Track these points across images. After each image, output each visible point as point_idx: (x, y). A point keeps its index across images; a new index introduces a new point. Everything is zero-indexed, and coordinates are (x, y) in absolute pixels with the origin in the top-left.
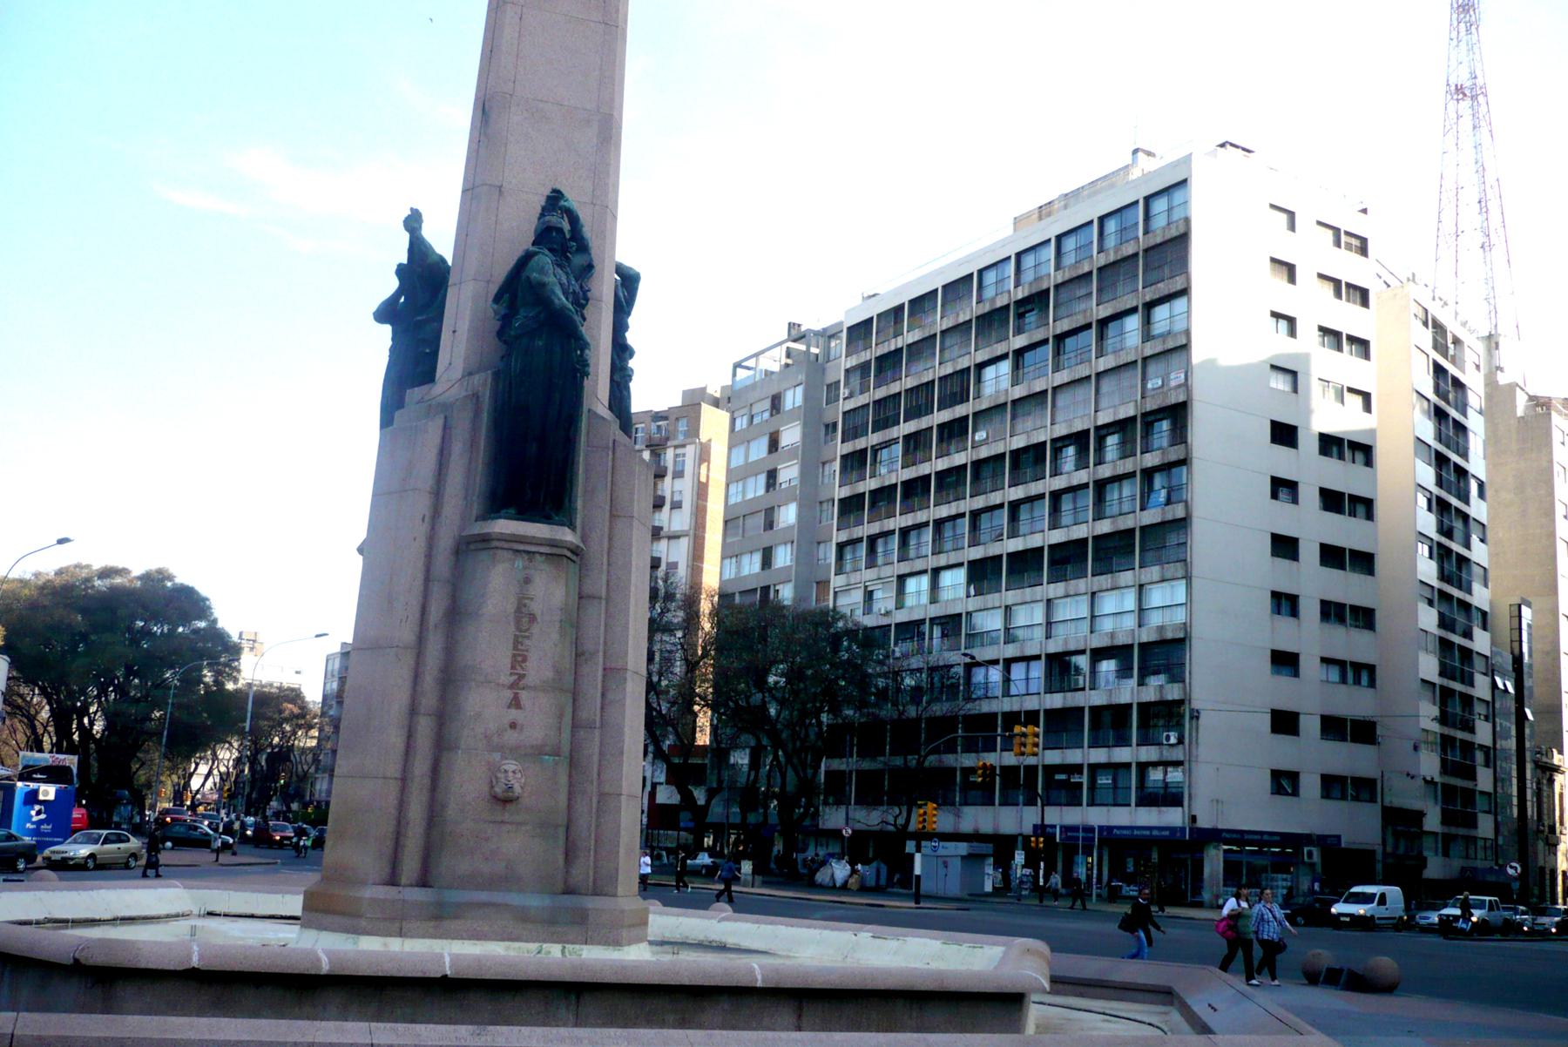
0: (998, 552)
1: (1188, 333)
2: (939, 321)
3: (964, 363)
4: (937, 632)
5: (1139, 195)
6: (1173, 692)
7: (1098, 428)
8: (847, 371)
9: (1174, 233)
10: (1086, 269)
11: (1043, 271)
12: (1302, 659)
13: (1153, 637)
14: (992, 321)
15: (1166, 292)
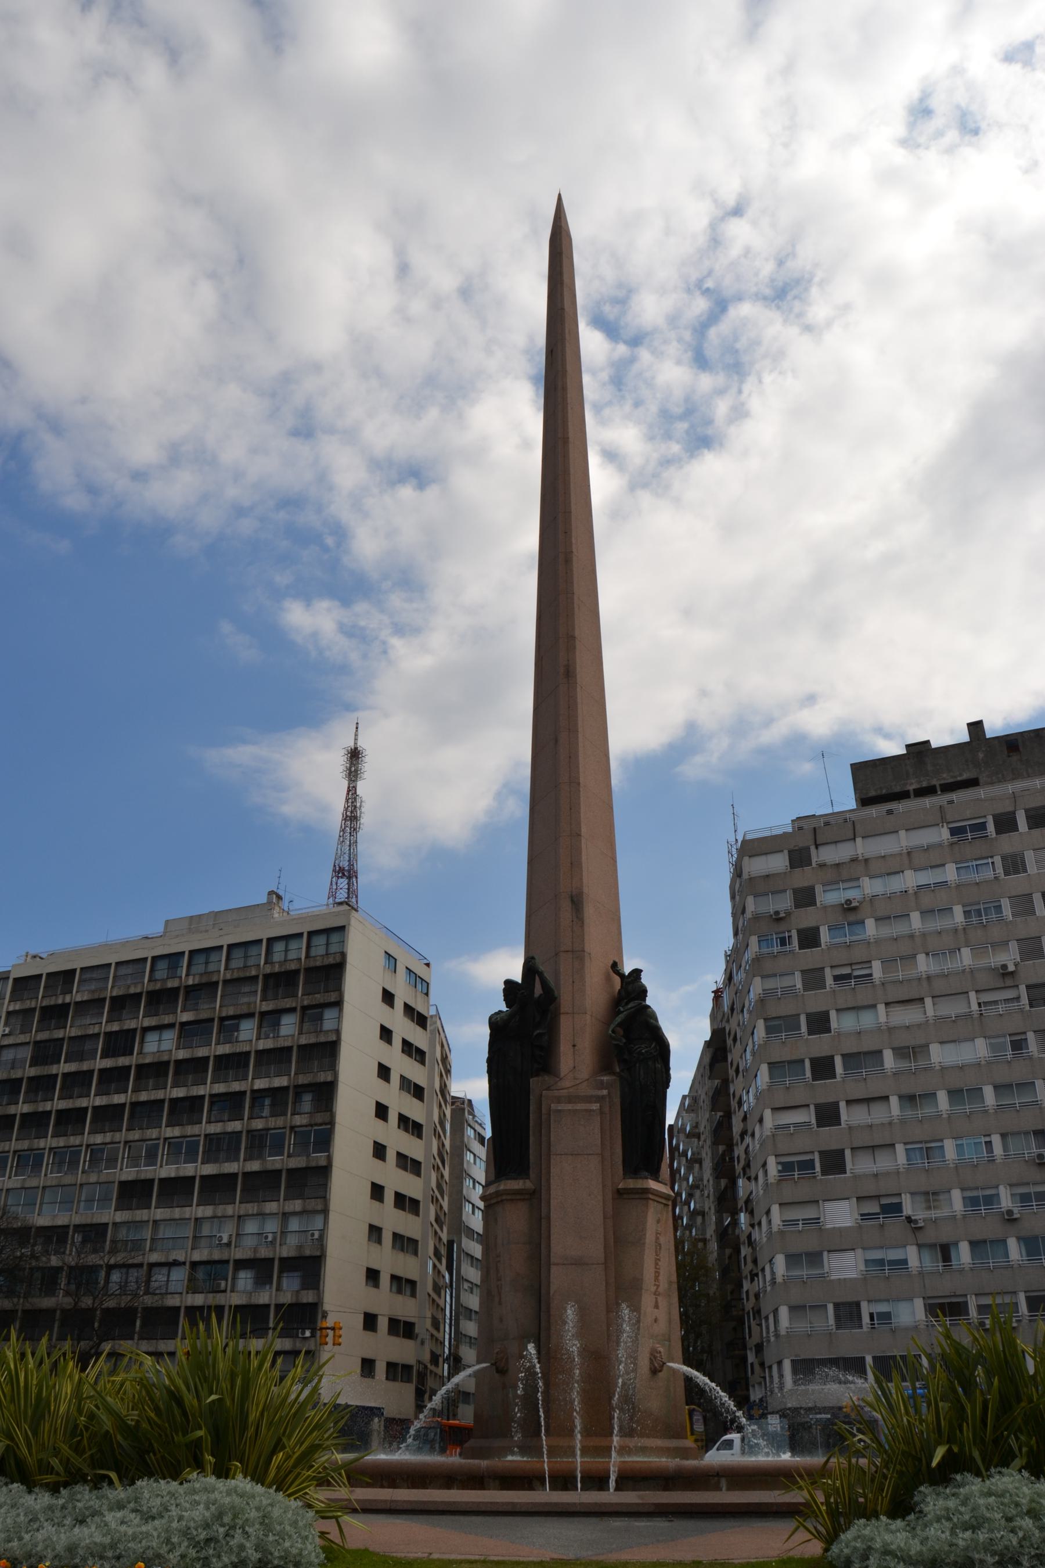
0: (149, 1176)
1: (338, 1032)
3: (131, 1024)
4: (78, 1238)
5: (305, 929)
6: (308, 1297)
8: (9, 1013)
9: (331, 960)
10: (254, 973)
11: (212, 968)
12: (382, 1274)
13: (292, 1254)
15: (322, 1001)
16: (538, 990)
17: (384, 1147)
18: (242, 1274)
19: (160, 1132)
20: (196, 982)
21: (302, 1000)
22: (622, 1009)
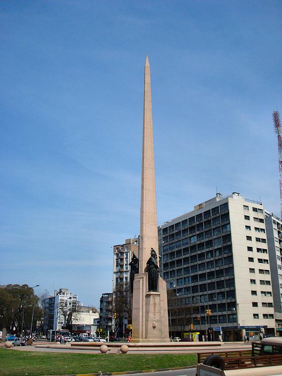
1: (230, 231)
2: (181, 228)
6: (233, 300)
14: (192, 229)
17: (253, 258)
18: (219, 296)
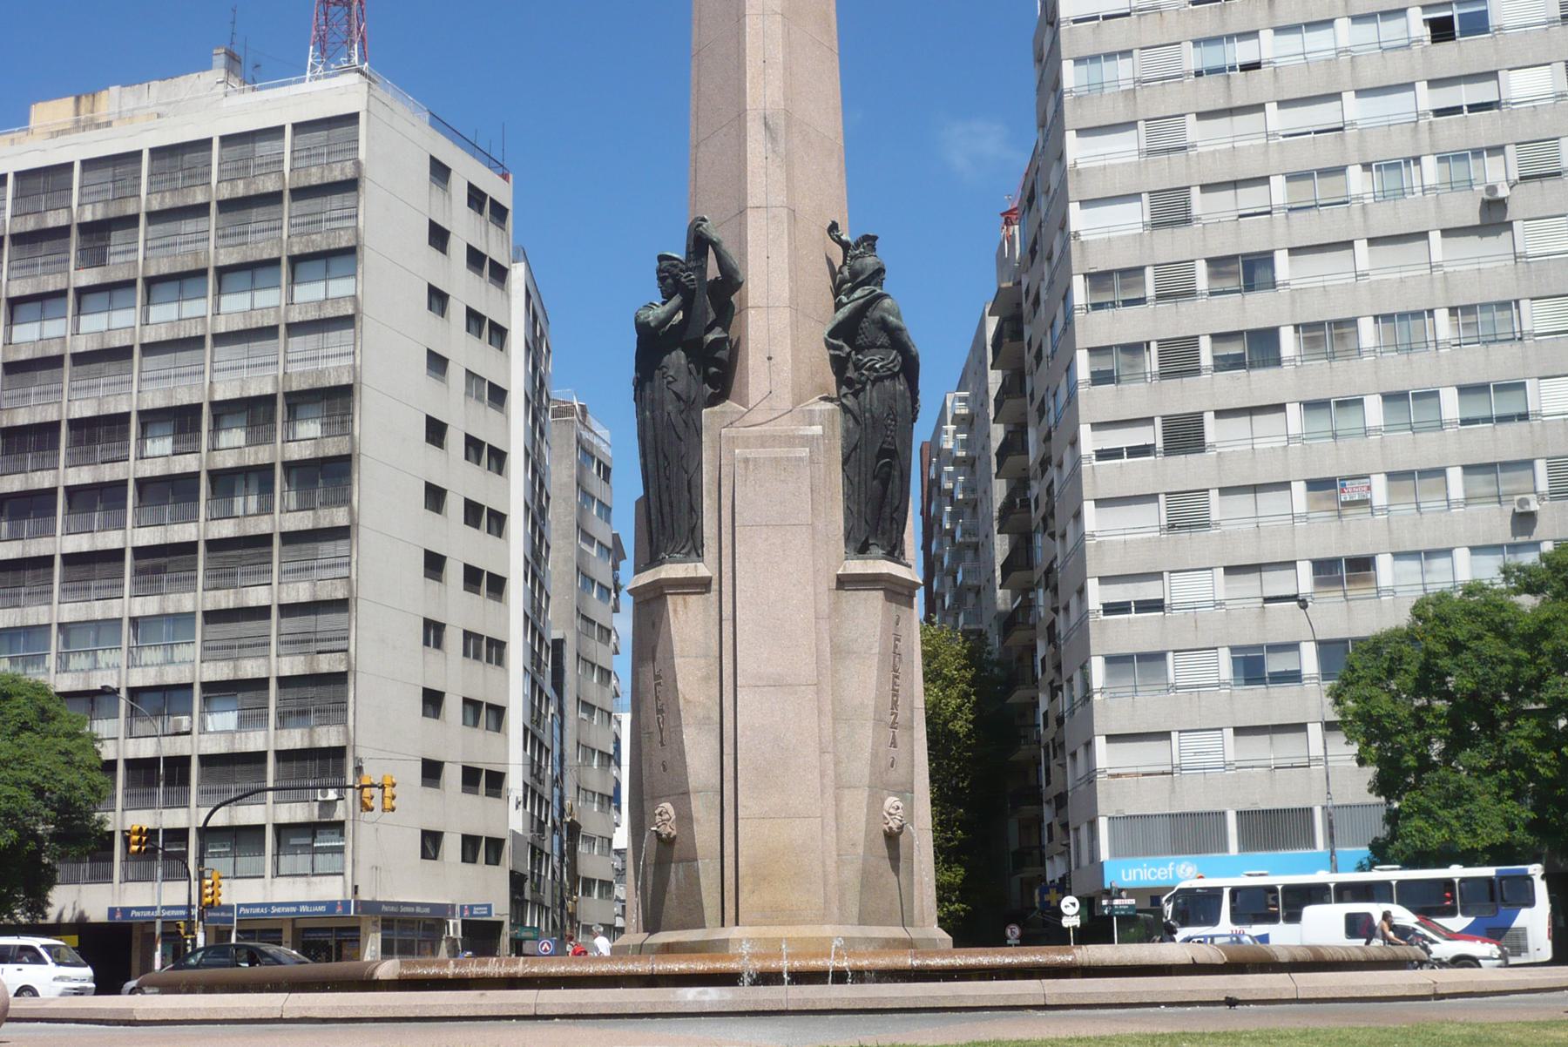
7: (214, 405)
12: (447, 697)
15: (325, 247)
16: (713, 272)
19: (57, 477)
20: (99, 216)
21: (290, 245)
22: (845, 299)
